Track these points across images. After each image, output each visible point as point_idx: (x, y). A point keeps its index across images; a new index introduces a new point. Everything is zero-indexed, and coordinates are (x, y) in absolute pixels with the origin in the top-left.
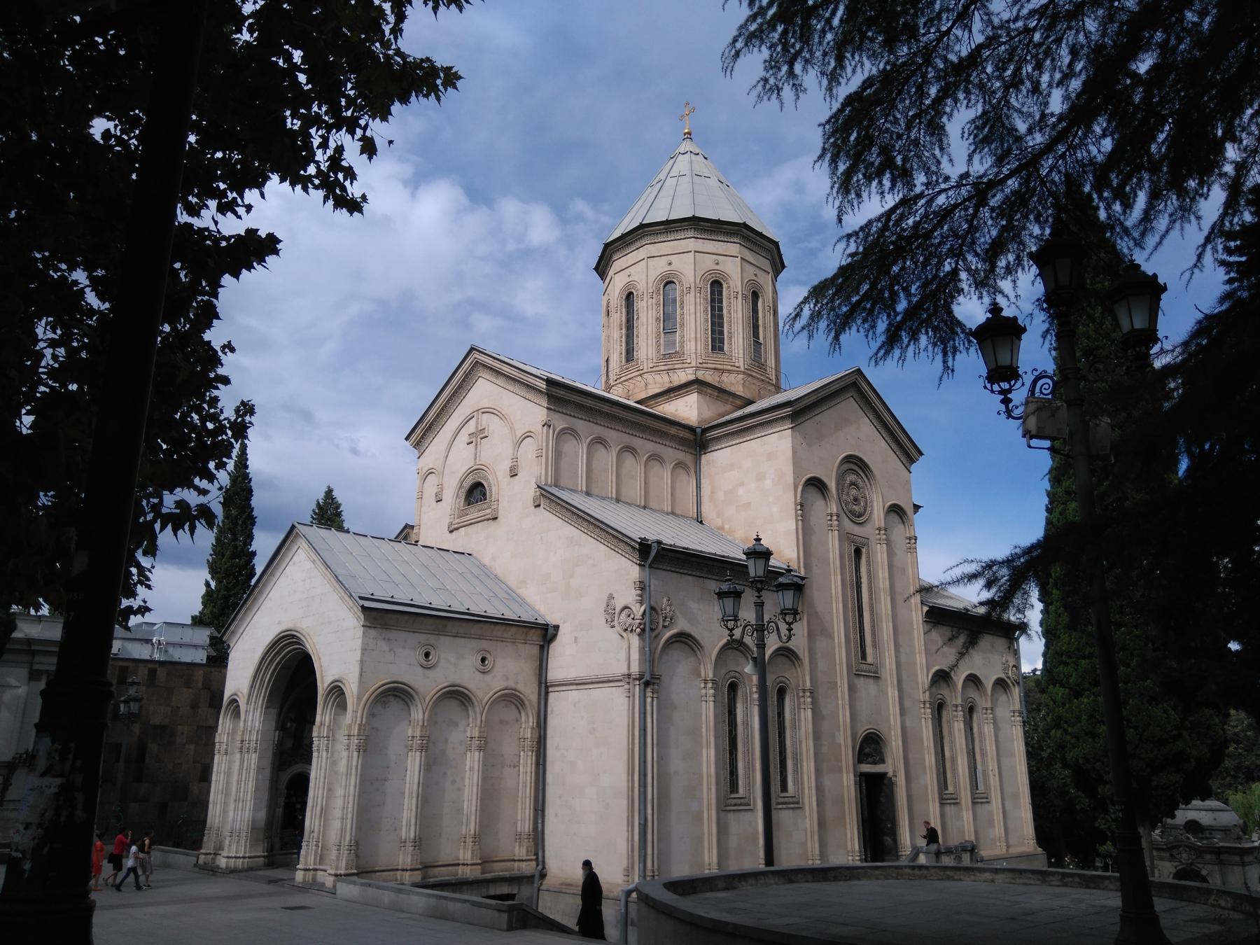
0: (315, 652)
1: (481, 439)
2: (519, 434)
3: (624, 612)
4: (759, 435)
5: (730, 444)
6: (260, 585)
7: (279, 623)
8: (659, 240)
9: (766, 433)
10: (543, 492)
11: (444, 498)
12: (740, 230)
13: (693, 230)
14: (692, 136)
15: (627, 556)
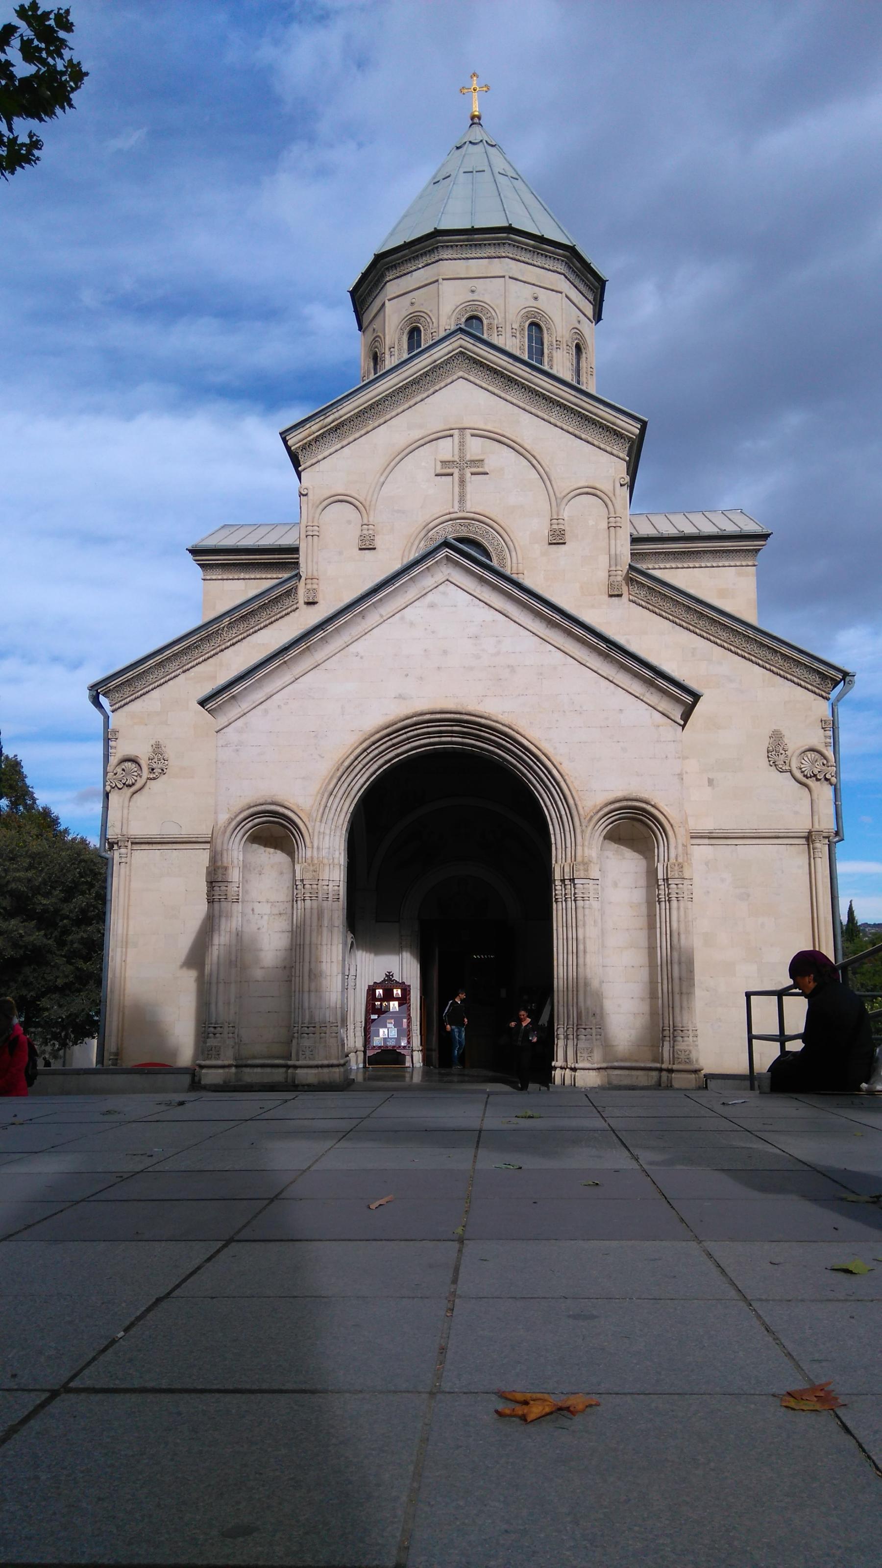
0: (545, 751)
1: (472, 474)
2: (563, 485)
3: (809, 754)
4: (709, 564)
5: (662, 566)
6: (330, 628)
7: (400, 697)
8: (522, 259)
9: (720, 564)
10: (641, 578)
11: (378, 543)
12: (597, 289)
13: (564, 264)
14: (481, 122)
15: (810, 687)
